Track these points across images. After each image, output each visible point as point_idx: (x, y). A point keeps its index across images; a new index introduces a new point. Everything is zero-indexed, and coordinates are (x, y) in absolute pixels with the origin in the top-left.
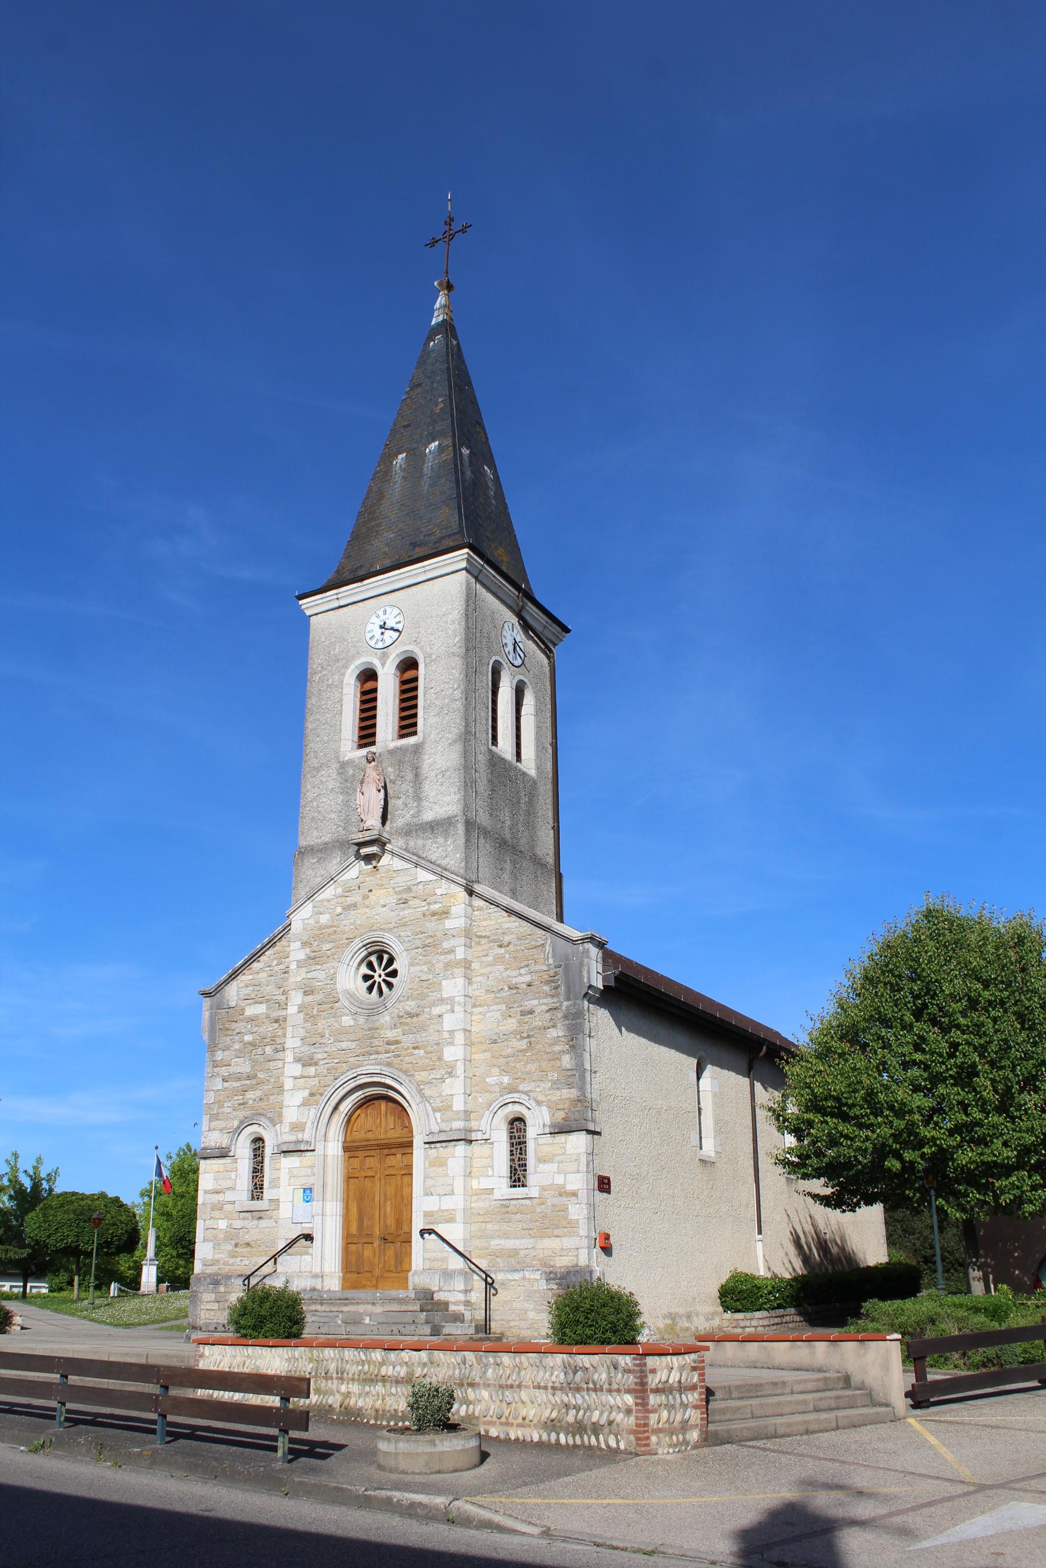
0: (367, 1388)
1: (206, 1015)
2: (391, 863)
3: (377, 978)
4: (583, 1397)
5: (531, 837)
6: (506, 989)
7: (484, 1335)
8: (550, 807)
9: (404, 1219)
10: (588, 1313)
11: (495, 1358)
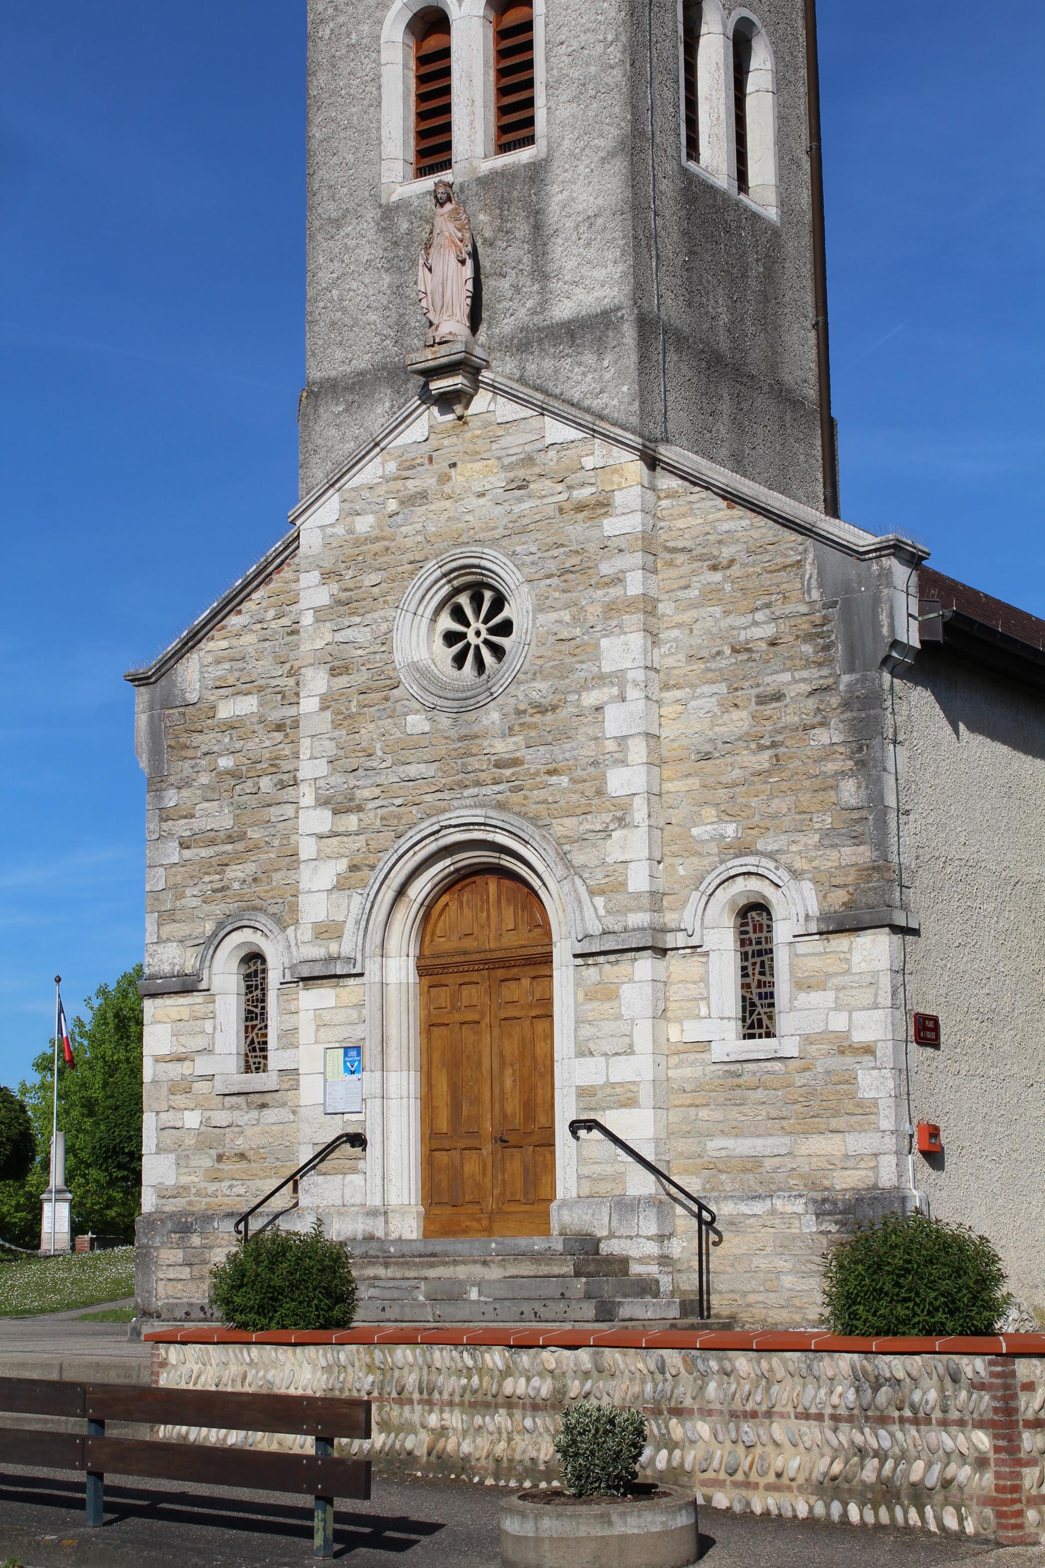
0: (478, 1420)
1: (142, 720)
2: (492, 408)
4: (892, 1435)
5: (772, 346)
6: (728, 651)
7: (699, 1320)
8: (809, 283)
9: (539, 1101)
10: (899, 1276)
11: (720, 1360)
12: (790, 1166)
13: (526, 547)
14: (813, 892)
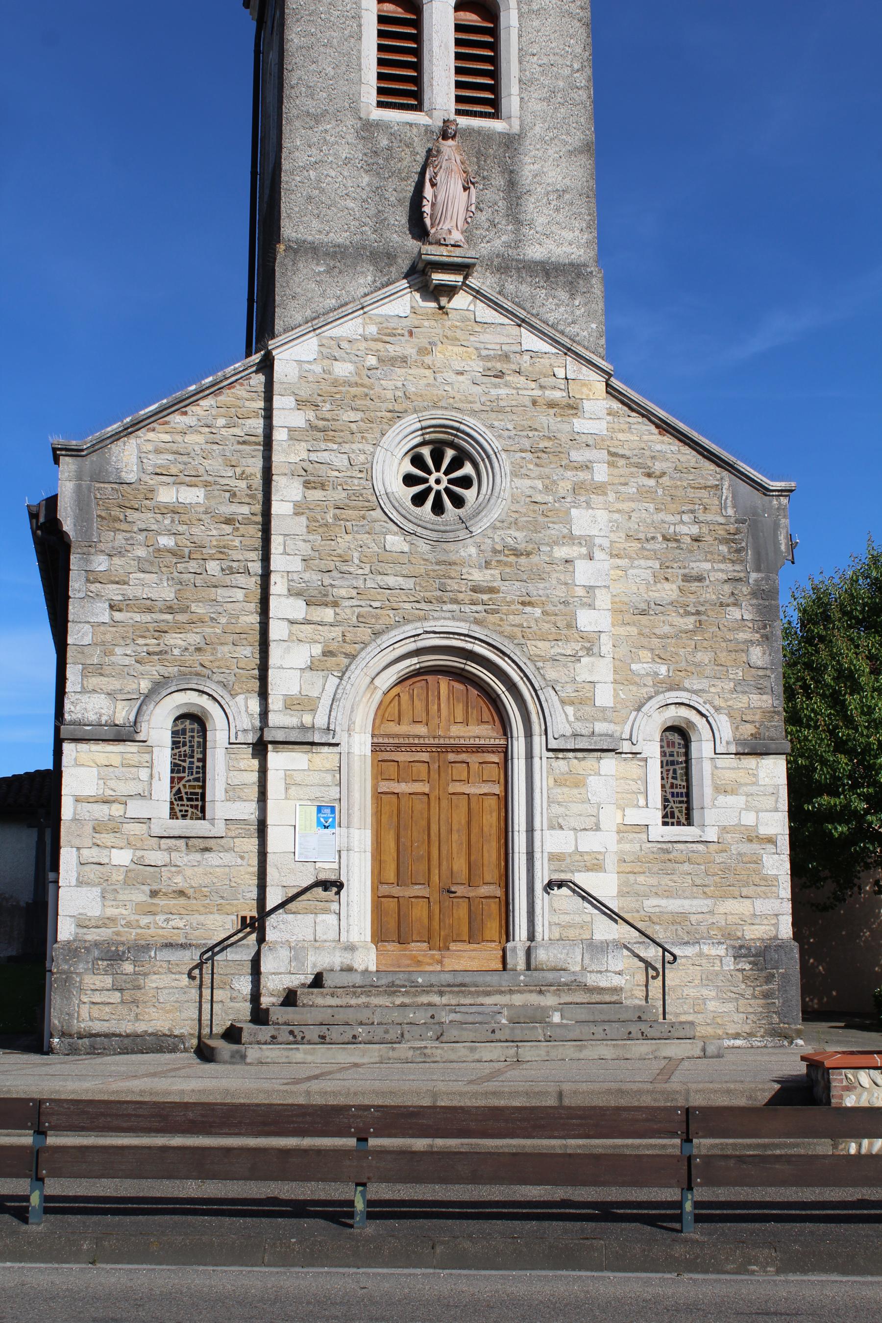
2: (472, 307)
3: (444, 484)
6: (660, 539)
9: (486, 862)
12: (711, 921)
13: (503, 423)
14: (729, 723)
